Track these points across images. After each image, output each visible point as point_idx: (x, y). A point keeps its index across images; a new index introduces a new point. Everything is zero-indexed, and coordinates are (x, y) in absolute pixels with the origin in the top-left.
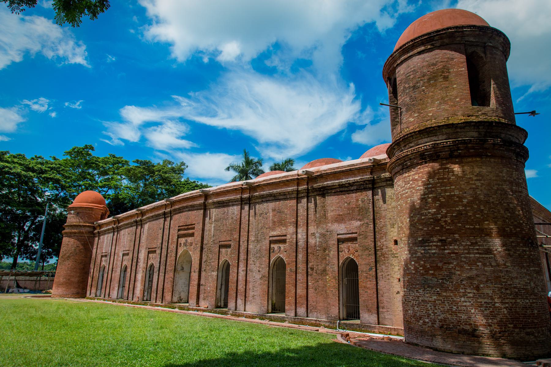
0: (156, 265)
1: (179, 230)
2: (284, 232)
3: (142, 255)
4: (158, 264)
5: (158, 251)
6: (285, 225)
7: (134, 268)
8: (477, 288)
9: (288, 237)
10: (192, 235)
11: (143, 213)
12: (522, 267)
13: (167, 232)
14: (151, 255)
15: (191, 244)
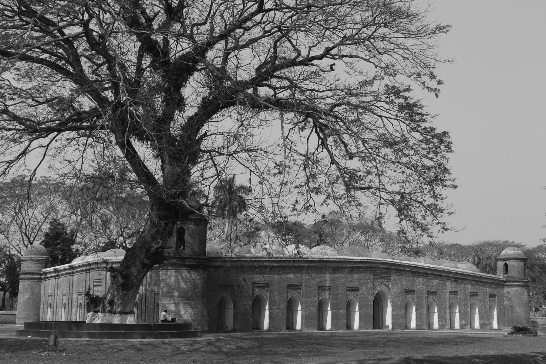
1: (94, 282)
3: (75, 296)
7: (70, 305)
10: (101, 285)
11: (73, 268)
13: (88, 283)
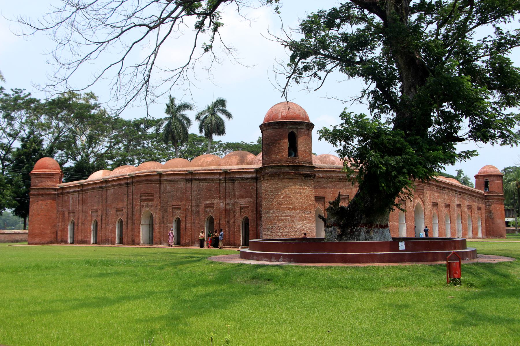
0: (124, 220)
1: (141, 196)
2: (213, 202)
4: (126, 220)
5: (125, 211)
8: (283, 229)
9: (215, 205)
10: (152, 200)
12: (300, 221)
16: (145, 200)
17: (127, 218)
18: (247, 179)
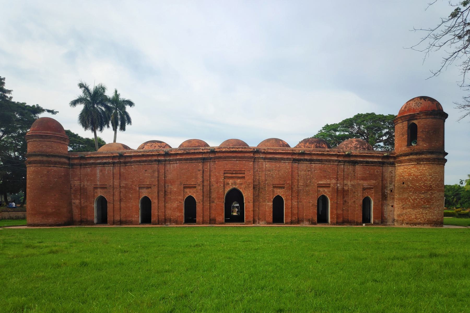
2: (329, 182)
6: (330, 178)
14: (187, 190)
15: (241, 184)
16: (232, 178)
17: (203, 196)
18: (372, 162)
